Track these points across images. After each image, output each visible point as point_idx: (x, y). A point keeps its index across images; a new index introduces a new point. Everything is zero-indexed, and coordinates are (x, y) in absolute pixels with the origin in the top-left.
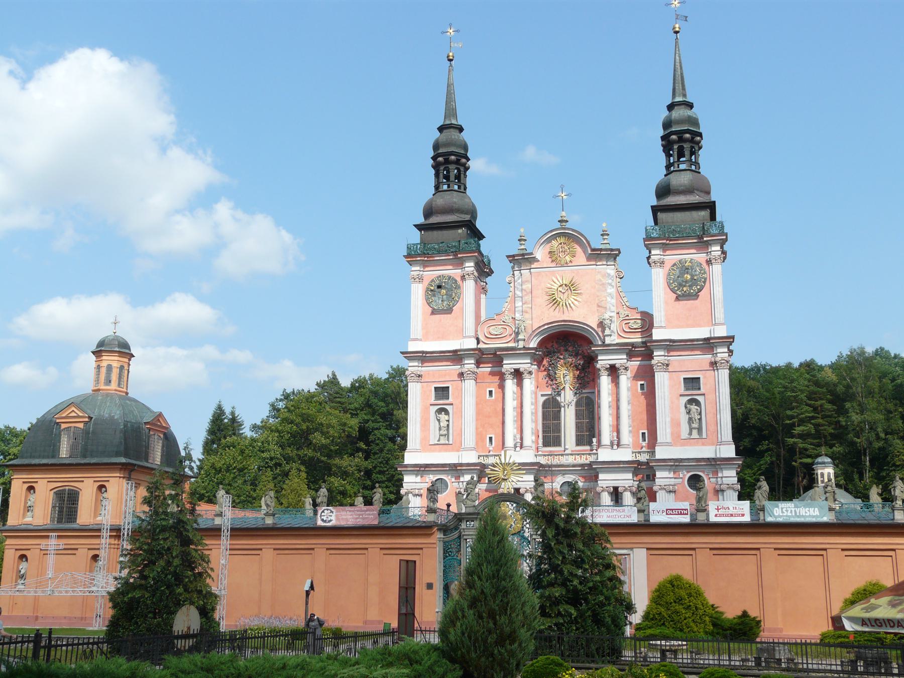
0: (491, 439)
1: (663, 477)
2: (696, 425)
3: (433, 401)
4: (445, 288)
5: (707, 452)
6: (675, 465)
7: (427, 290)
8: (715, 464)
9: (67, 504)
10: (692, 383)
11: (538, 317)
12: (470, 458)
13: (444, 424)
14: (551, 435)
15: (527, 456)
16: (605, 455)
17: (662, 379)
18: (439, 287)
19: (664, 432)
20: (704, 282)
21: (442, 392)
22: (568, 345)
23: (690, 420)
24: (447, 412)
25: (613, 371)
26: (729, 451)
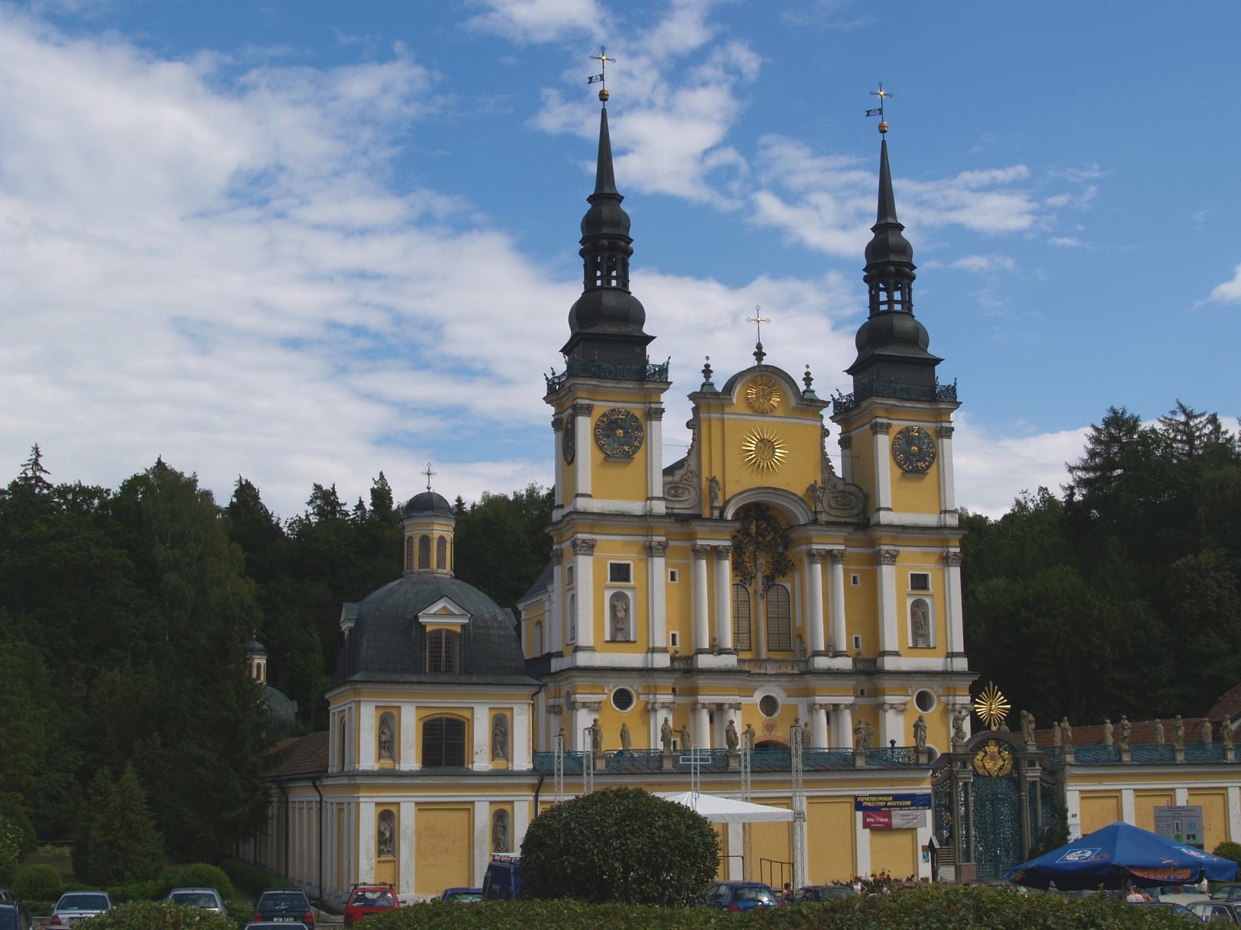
0: (674, 636)
3: (608, 582)
4: (621, 428)
5: (935, 663)
7: (597, 427)
9: (445, 745)
10: (920, 582)
11: (738, 482)
17: (888, 574)
19: (891, 641)
20: (933, 458)
21: (620, 572)
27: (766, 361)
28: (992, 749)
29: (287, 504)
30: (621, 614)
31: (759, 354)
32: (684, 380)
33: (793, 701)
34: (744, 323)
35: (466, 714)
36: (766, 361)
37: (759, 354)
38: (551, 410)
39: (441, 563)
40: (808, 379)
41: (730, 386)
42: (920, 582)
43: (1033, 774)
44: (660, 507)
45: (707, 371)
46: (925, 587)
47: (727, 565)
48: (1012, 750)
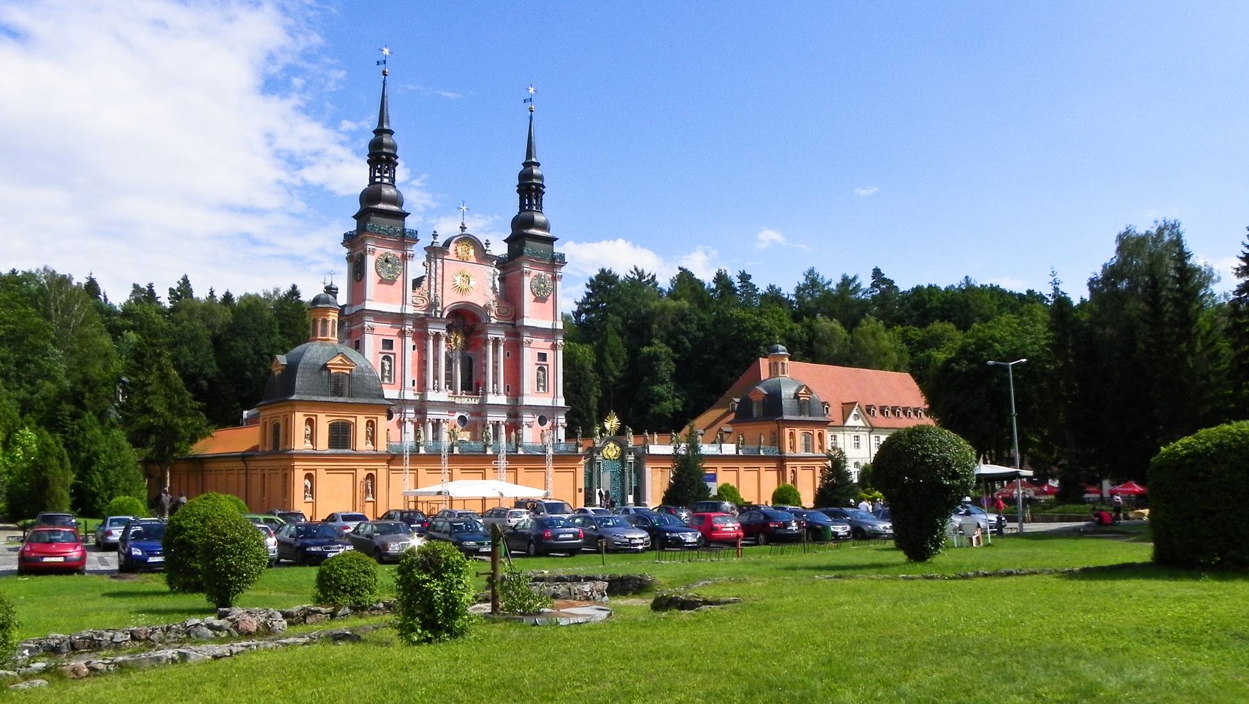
1: (527, 418)
2: (542, 383)
6: (533, 409)
8: (554, 410)
9: (341, 435)
10: (543, 357)
11: (450, 299)
12: (410, 395)
13: (387, 368)
14: (450, 383)
15: (444, 396)
16: (492, 399)
18: (387, 261)
22: (465, 321)
23: (538, 381)
24: (388, 359)
25: (496, 342)
26: (561, 402)
27: (466, 231)
28: (611, 445)
29: (117, 296)
30: (387, 368)
31: (463, 228)
32: (425, 240)
33: (474, 419)
34: (457, 208)
35: (353, 420)
36: (466, 231)
37: (463, 228)
38: (346, 250)
39: (333, 334)
40: (487, 244)
41: (447, 244)
42: (543, 357)
43: (631, 458)
44: (410, 310)
45: (435, 235)
46: (545, 359)
47: (443, 343)
48: (621, 446)
